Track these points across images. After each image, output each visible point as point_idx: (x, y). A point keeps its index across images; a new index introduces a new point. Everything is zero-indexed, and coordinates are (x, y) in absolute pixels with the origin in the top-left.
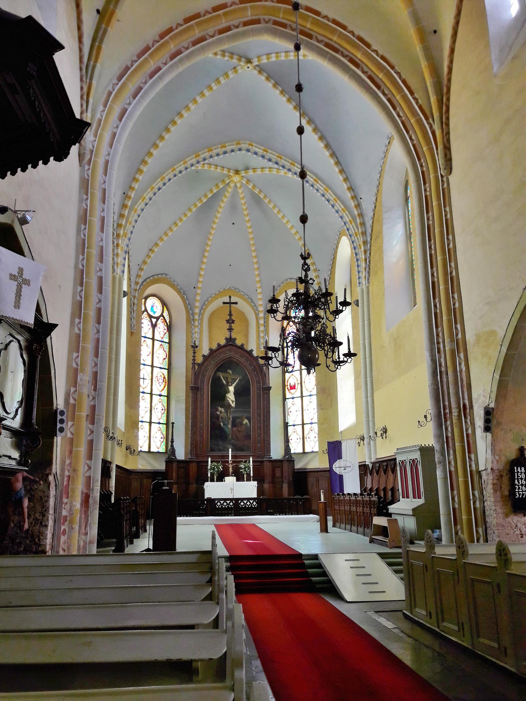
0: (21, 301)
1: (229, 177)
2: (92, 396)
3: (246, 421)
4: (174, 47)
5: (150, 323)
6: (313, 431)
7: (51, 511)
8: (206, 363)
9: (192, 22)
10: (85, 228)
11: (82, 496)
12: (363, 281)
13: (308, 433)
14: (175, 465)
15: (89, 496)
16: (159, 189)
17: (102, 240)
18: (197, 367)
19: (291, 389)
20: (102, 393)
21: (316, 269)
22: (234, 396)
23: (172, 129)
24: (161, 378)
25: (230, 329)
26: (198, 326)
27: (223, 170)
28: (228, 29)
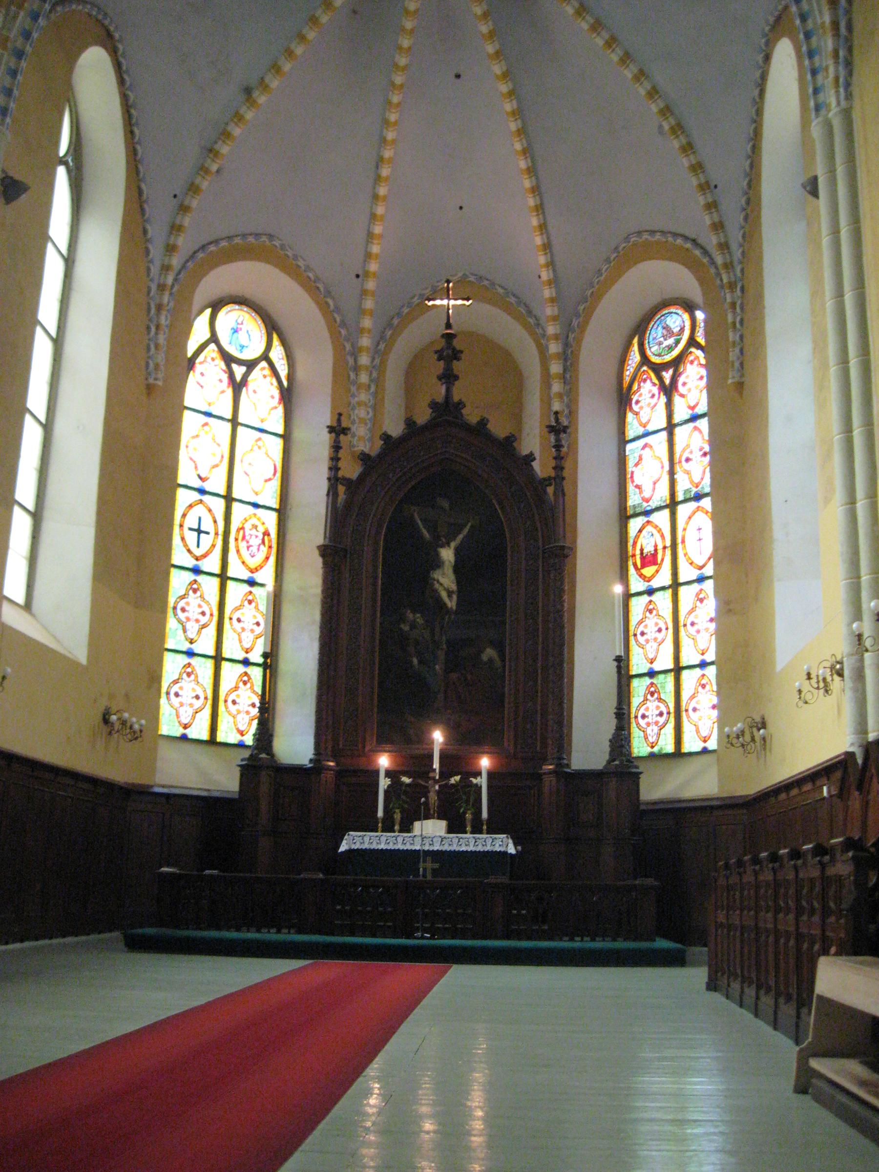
3: (489, 653)
5: (225, 377)
6: (708, 687)
12: (830, 97)
13: (693, 697)
14: (265, 777)
18: (341, 489)
19: (643, 566)
21: (707, 183)
22: (452, 577)
24: (254, 532)
25: (449, 378)
26: (369, 387)
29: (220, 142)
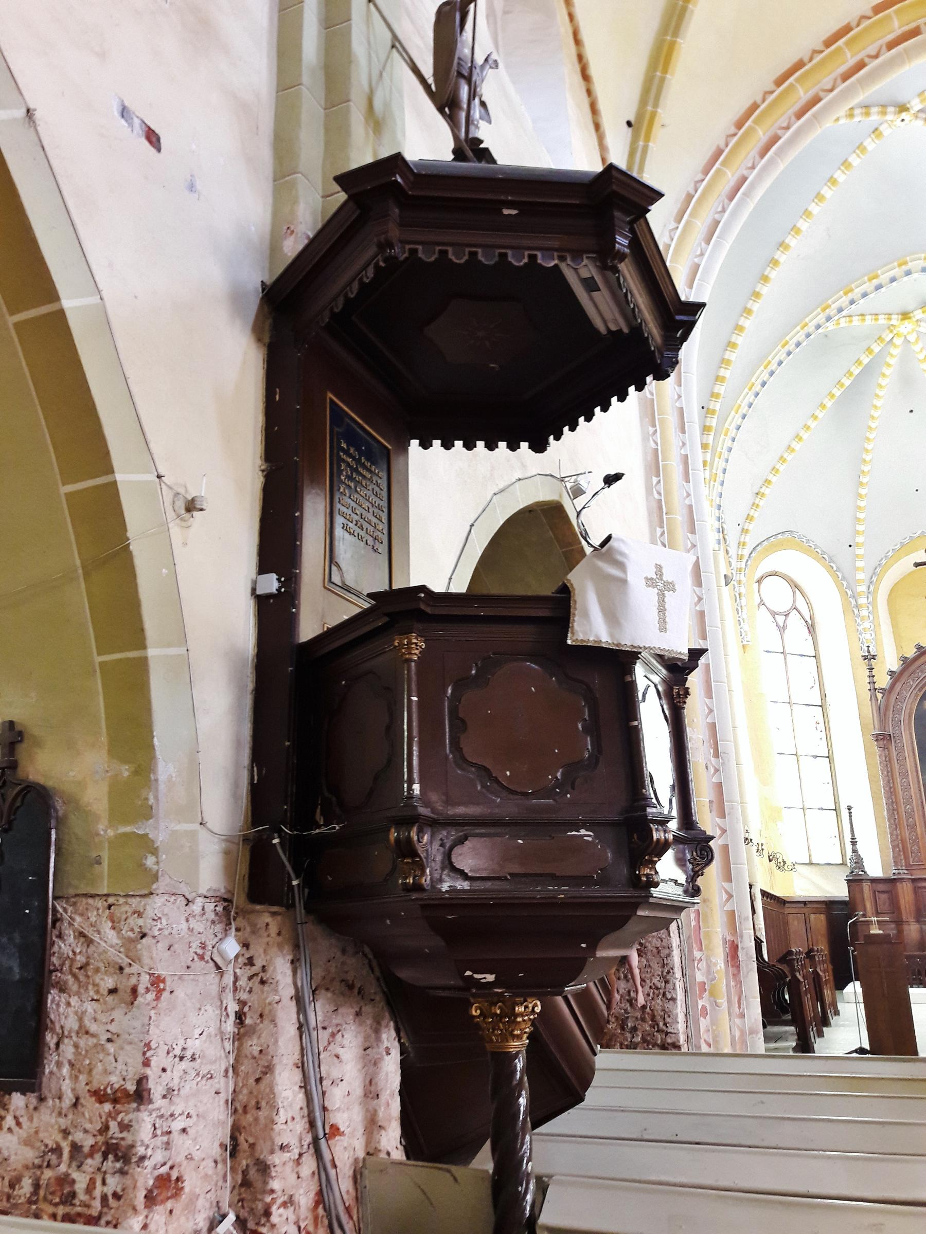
0: (667, 620)
1: (890, 328)
2: (713, 766)
4: (764, 134)
7: (678, 974)
8: (898, 687)
9: (791, 80)
10: (659, 481)
11: (724, 948)
15: (737, 946)
16: (764, 384)
17: (689, 495)
18: (879, 696)
20: (728, 761)
23: (773, 275)
27: (877, 320)
28: (861, 65)
29: (764, 487)
